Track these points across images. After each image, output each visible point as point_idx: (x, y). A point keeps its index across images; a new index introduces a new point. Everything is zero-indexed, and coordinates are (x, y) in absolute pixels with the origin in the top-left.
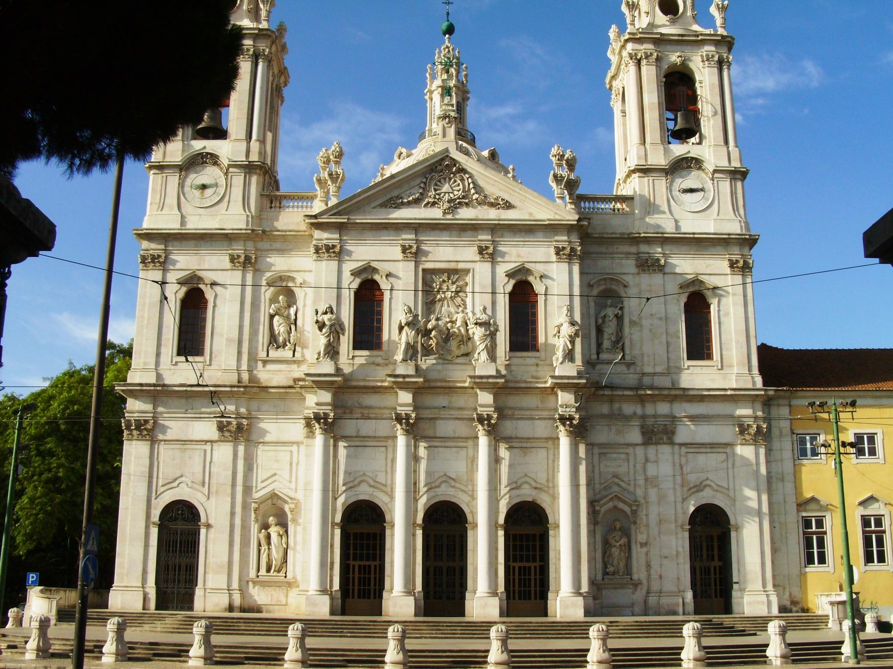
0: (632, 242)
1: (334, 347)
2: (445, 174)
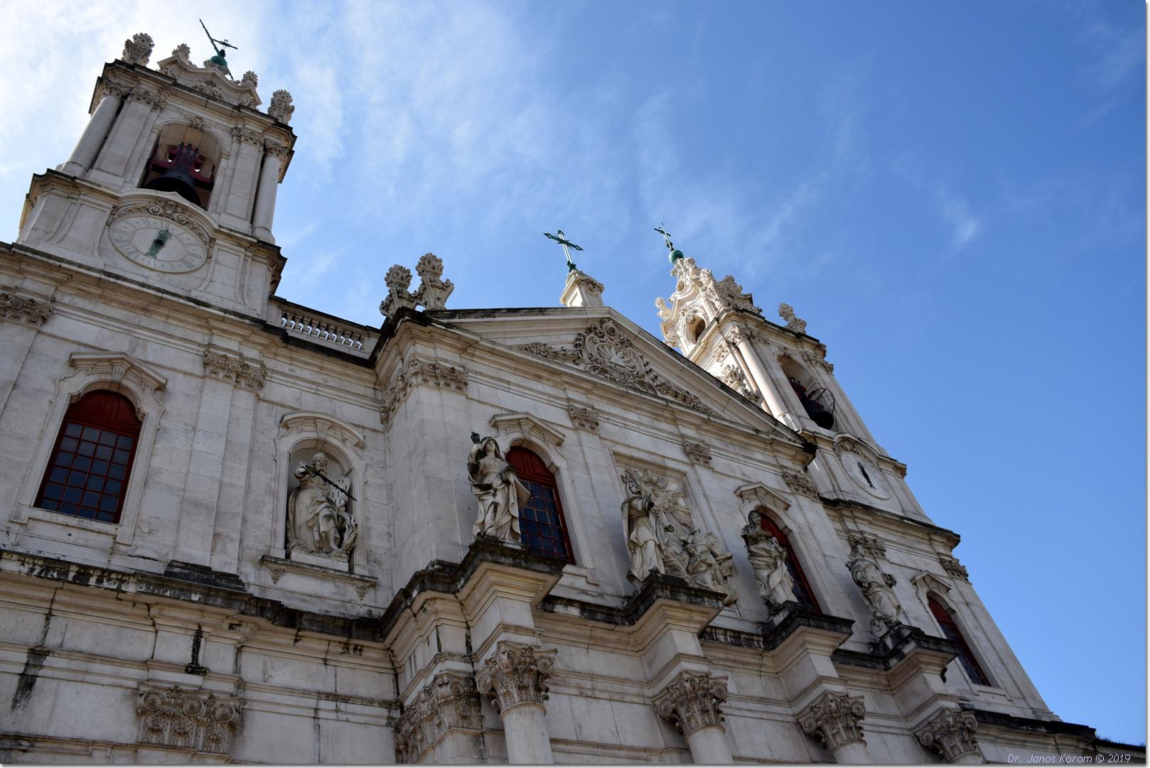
0: (834, 517)
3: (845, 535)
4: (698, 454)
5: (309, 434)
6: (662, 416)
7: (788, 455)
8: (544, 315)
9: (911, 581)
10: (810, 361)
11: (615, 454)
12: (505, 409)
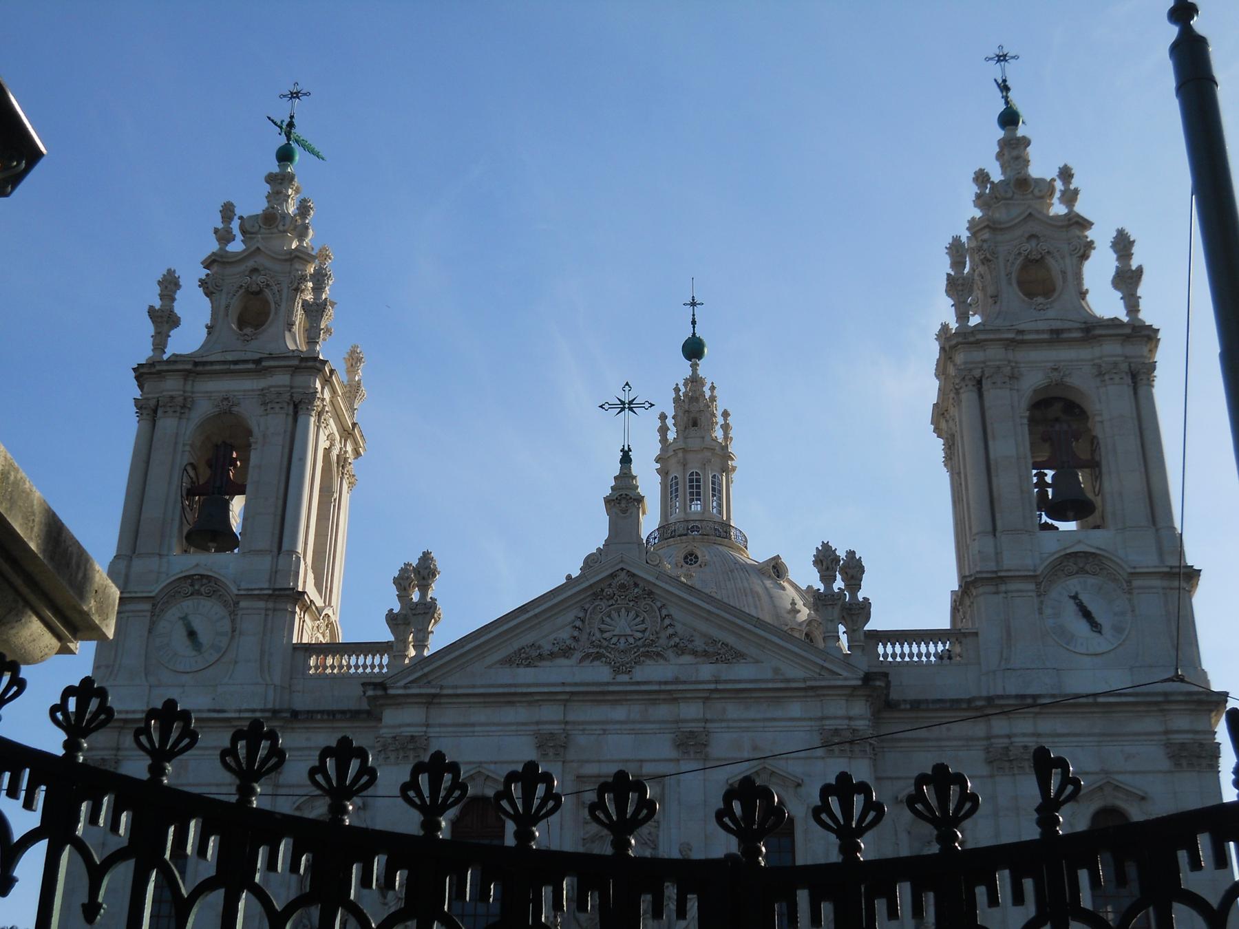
2: (619, 602)
3: (985, 743)
6: (659, 699)
8: (528, 612)
10: (1100, 374)
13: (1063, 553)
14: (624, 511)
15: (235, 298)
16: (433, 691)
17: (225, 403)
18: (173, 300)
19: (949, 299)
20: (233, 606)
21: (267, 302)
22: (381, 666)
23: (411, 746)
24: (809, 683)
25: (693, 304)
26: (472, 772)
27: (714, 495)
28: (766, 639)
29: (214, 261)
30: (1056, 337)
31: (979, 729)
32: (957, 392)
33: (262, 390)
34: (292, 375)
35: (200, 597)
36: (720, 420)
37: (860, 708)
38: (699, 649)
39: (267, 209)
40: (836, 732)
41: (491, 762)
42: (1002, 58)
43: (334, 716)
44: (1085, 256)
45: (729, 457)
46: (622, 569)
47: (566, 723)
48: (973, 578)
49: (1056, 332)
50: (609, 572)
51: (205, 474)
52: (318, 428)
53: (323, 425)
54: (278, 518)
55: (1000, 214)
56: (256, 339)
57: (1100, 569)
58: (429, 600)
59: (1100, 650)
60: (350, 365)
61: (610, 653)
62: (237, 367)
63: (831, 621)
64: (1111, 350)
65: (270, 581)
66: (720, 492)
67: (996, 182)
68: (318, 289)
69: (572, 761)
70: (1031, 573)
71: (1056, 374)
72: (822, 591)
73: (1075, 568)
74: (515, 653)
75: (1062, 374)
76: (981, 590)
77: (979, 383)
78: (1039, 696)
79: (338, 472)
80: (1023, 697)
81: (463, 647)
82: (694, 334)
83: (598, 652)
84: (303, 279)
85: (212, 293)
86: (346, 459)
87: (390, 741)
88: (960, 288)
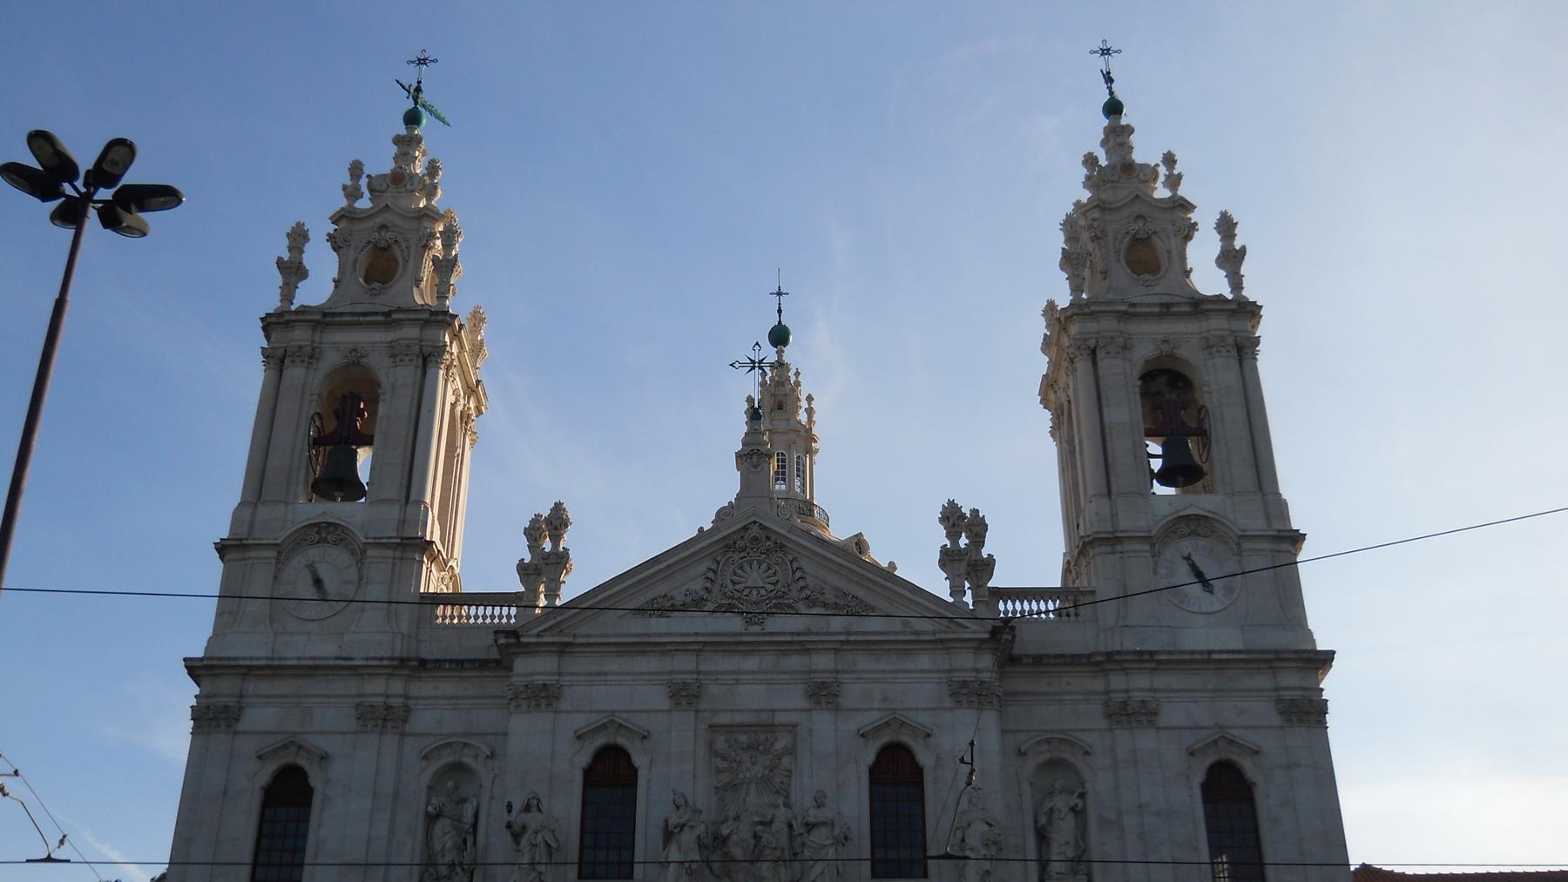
0: (1095, 672)
1: (540, 873)
3: (1103, 697)
4: (823, 694)
5: (447, 758)
6: (791, 650)
7: (968, 648)
9: (1187, 750)
10: (1209, 347)
11: (711, 726)
12: (597, 712)
13: (1175, 516)
14: (755, 467)
15: (363, 253)
16: (566, 639)
17: (353, 354)
18: (302, 252)
19: (1063, 273)
20: (360, 554)
21: (395, 260)
22: (509, 616)
23: (543, 694)
24: (938, 636)
25: (779, 294)
26: (605, 721)
27: (798, 476)
28: (896, 592)
29: (343, 217)
30: (1166, 311)
31: (1098, 684)
32: (1072, 361)
33: (391, 342)
34: (421, 328)
35: (326, 545)
36: (804, 404)
37: (986, 661)
38: (830, 602)
39: (394, 169)
40: (965, 684)
41: (624, 711)
42: (1106, 52)
43: (462, 665)
44: (1188, 237)
45: (813, 439)
46: (755, 522)
47: (699, 673)
48: (1091, 538)
49: (1168, 305)
50: (742, 524)
51: (331, 425)
52: (446, 381)
53: (451, 379)
54: (407, 468)
55: (1107, 195)
56: (384, 293)
57: (1212, 532)
58: (562, 550)
59: (1210, 610)
60: (472, 325)
61: (742, 604)
62: (367, 319)
63: (958, 576)
64: (1217, 324)
65: (398, 530)
66: (804, 472)
67: (1103, 165)
68: (448, 245)
69: (705, 710)
70: (1146, 534)
71: (1166, 346)
72: (949, 546)
73: (1188, 530)
74: (648, 602)
75: (1172, 346)
76: (1098, 550)
77: (1094, 352)
78: (1156, 652)
79: (462, 430)
80: (1141, 653)
81: (596, 596)
82: (780, 322)
83: (730, 604)
84: (432, 236)
85: (340, 247)
86: (469, 416)
87: (521, 689)
88: (1075, 262)
